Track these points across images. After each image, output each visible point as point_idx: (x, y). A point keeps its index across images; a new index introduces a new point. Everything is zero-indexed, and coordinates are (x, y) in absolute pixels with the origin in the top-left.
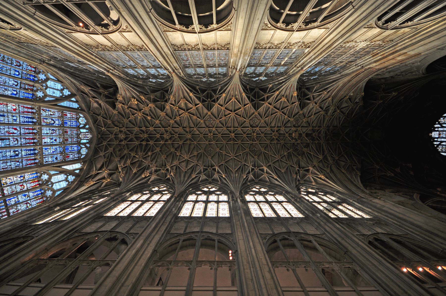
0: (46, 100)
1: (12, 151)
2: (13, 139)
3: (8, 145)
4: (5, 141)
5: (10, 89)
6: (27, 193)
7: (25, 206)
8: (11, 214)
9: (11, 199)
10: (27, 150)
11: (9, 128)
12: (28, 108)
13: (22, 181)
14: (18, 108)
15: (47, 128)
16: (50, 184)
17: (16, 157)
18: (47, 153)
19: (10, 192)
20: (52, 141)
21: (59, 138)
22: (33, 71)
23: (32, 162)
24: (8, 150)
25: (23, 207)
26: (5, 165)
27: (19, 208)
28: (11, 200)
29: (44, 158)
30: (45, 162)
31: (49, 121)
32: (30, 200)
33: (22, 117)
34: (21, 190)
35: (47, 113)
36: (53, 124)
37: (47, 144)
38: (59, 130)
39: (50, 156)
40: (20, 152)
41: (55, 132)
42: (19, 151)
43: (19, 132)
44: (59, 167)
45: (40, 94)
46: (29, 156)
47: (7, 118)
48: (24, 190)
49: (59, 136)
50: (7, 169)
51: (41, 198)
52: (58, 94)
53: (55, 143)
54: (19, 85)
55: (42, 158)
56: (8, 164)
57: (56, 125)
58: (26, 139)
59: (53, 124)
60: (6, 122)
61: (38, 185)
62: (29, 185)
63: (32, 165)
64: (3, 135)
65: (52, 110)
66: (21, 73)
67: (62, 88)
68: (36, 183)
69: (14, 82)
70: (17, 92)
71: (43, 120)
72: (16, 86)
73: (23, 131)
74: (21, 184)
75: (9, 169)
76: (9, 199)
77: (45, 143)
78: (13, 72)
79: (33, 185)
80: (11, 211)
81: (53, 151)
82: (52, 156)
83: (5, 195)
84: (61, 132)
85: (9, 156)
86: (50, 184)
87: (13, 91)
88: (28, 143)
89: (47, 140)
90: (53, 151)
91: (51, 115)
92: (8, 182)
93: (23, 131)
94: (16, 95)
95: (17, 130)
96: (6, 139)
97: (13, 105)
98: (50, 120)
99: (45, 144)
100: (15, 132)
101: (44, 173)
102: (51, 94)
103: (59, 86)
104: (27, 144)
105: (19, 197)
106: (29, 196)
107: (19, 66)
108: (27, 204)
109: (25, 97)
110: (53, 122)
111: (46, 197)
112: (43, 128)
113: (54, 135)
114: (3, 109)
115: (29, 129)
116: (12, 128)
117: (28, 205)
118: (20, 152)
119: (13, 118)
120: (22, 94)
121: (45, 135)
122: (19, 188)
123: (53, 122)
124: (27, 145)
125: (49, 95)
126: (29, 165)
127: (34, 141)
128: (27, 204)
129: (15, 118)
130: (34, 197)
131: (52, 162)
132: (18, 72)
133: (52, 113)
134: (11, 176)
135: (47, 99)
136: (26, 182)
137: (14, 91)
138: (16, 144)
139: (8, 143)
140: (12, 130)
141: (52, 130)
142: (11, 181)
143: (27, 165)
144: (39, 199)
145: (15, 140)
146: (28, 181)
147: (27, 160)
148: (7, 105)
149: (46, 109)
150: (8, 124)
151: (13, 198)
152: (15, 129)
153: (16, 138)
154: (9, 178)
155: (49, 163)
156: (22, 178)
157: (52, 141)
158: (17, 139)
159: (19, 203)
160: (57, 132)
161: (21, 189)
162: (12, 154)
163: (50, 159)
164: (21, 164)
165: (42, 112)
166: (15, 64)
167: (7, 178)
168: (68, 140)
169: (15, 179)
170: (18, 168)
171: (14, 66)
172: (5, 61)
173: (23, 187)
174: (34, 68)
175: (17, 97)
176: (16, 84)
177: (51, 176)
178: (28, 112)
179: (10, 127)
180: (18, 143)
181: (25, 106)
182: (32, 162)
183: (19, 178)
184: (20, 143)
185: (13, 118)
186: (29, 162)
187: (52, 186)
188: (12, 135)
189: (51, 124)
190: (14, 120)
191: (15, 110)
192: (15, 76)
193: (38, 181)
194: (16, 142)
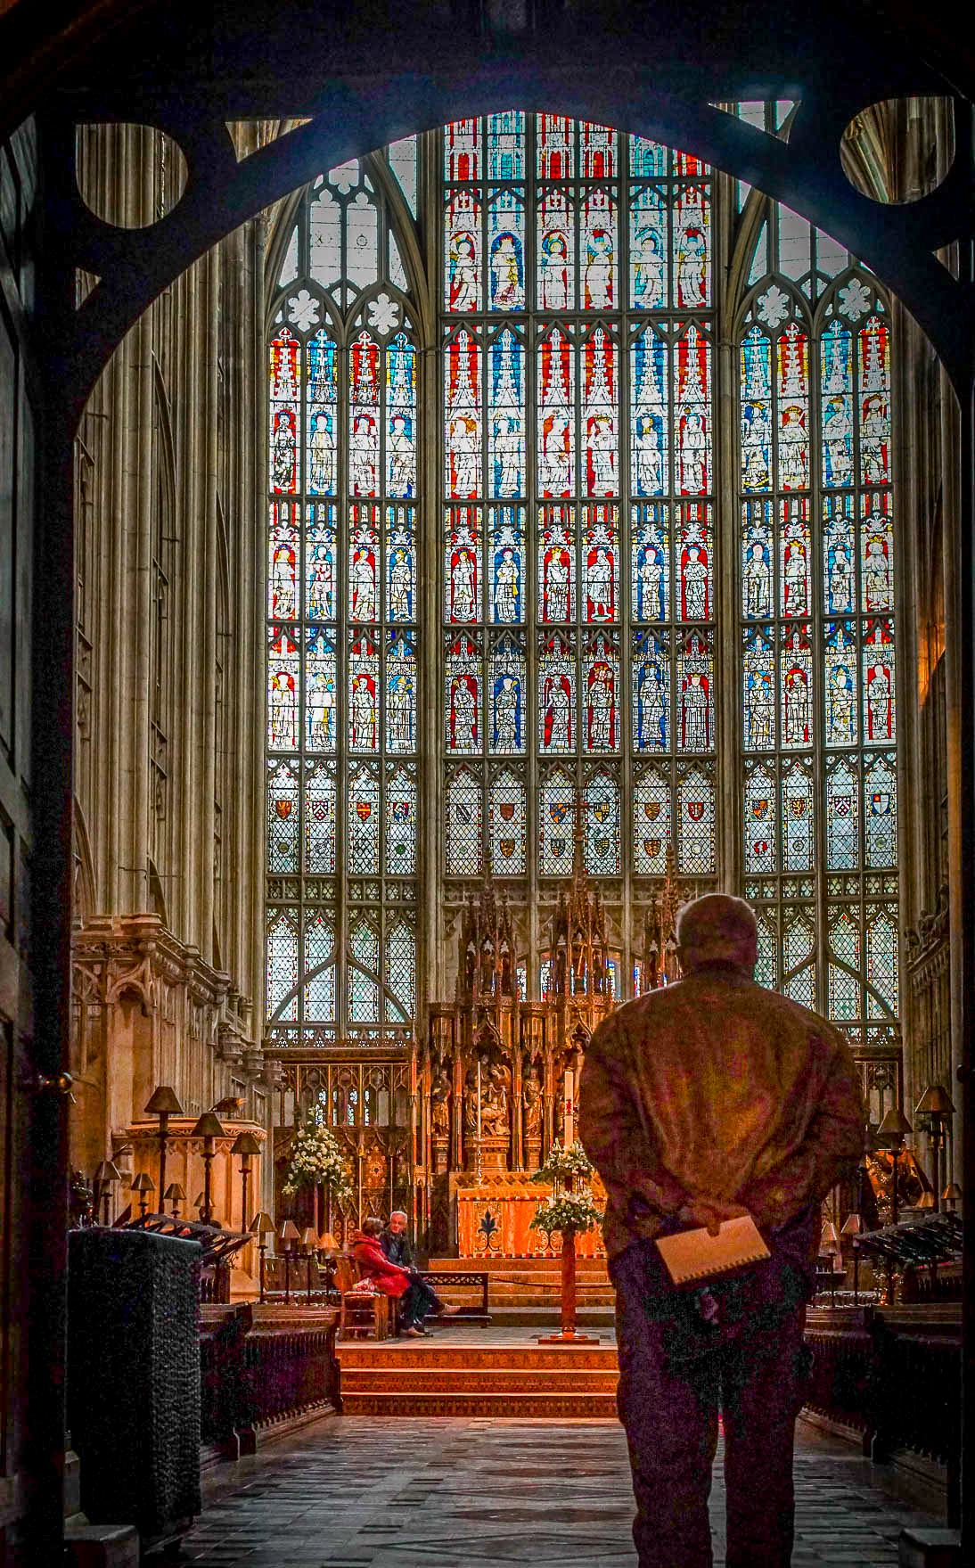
0: (404, 280)
1: (639, 443)
2: (589, 436)
3: (612, 458)
4: (595, 469)
5: (389, 446)
6: (825, 402)
7: (875, 418)
8: (888, 476)
9: (829, 466)
10: (638, 378)
11: (545, 452)
12: (455, 368)
13: (769, 412)
14: (459, 413)
15: (540, 277)
16: (814, 286)
17: (665, 426)
18: (661, 286)
19: (801, 469)
20: (601, 255)
21: (587, 211)
22: (293, 354)
23: (692, 359)
24: (634, 456)
25: (878, 430)
26: (691, 471)
27: (874, 442)
28: (834, 469)
29: (680, 301)
30: (703, 293)
31: (504, 264)
32: (855, 393)
33: (495, 395)
34: (807, 422)
35: (468, 276)
36: (514, 242)
37: (615, 283)
38: (544, 211)
39: (676, 266)
40: (643, 409)
41: (555, 236)
42: (640, 414)
43: (562, 411)
44: (737, 221)
45: (384, 315)
46: (665, 371)
47: (506, 456)
48: (806, 412)
49: (577, 211)
50: (709, 465)
51: (866, 343)
52: (365, 216)
53: (615, 234)
54: (365, 410)
55: (683, 315)
56: (689, 458)
57: (522, 226)
58: (589, 383)
59: (514, 242)
60: (523, 461)
61: (799, 349)
62: (793, 388)
63: (708, 361)
64: (573, 475)
65: (450, 246)
66: (316, 409)
67: (326, 195)
68: (793, 354)
69: (360, 431)
70: (397, 418)
71: (504, 297)
72: (372, 422)
73: (556, 396)
74: (780, 417)
75: (710, 457)
76: (828, 477)
77: (609, 289)
78: (322, 441)
79: (793, 370)
80: (875, 475)
81: (655, 251)
82: (676, 258)
83: (807, 486)
84: (556, 197)
85: (658, 454)
86: (814, 286)
87: (398, 432)
88: (608, 374)
89: (598, 281)
90: (655, 251)
91: (472, 254)
92: (765, 468)
93: (556, 396)
94: (408, 421)
95: (551, 419)
96: (590, 462)
97: (453, 430)
98: (499, 259)
99: (615, 291)
100: (559, 425)
101: (755, 308)
102: (375, 254)
103: (323, 212)
104: (610, 378)
105: (828, 435)
106: (840, 397)
107: (292, 418)
108: (867, 410)
109: (411, 379)
110: (507, 243)
111: (866, 317)
112: (540, 307)
113: (570, 246)
114: (473, 471)
115: (547, 367)
116: (545, 436)
117: (875, 404)
118: (643, 409)
119: (504, 432)
120: (400, 395)
121: (571, 291)
122: (794, 432)
123: (507, 243)
124: (615, 378)
125: (379, 270)
126: (704, 377)
127: (600, 346)
128: (867, 410)
129: (503, 426)
130: (850, 374)
131: (709, 255)
132: (315, 418)
133: (465, 248)
134: (739, 455)
135: (399, 279)
136: (774, 399)
137: (393, 429)
138: (611, 427)
139: (607, 455)
140: (555, 441)
141: (550, 253)
142: (759, 457)
143: (703, 382)
144: (866, 352)
145: (593, 429)
146: (773, 388)
147: (682, 382)
148: (453, 454)
149: (448, 281)
150: (531, 452)
151: (828, 460)
152: (549, 423)
153: (584, 425)
154: (744, 460)
155: (708, 275)
156: (756, 412)
157: (601, 255)
158: (591, 421)
159: (856, 440)
160: (558, 220)
161: (802, 423)
162: (650, 440)
163: (693, 269)
164: (697, 409)
165: (462, 306)
166: (289, 433)
167: (745, 470)
168: (599, 156)
169: (754, 439)
170: (709, 424)
171: (298, 435)
172: (288, 473)
173: (792, 415)
174: (278, 353)
175: (419, 415)
176: (364, 423)
177: (773, 278)
178: (473, 367)
179: (540, 446)
180: (607, 418)
181: (448, 379)
182: (692, 359)
183: (752, 423)
184: (607, 410)
185: (504, 432)
186: (693, 371)
187: (825, 279)
188: (572, 441)
189: (518, 253)
190: (510, 429)
191: (470, 426)
192: (335, 429)
193: (786, 341)
194: (603, 425)
